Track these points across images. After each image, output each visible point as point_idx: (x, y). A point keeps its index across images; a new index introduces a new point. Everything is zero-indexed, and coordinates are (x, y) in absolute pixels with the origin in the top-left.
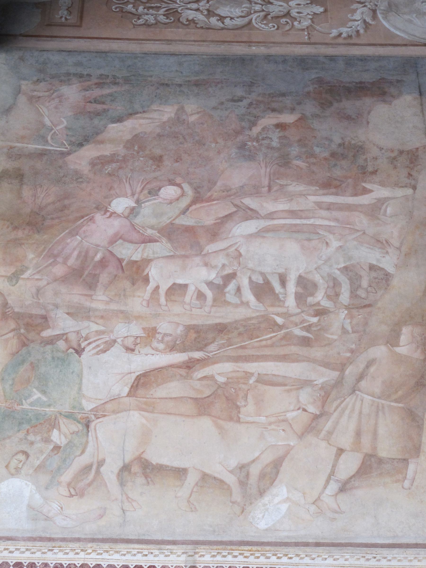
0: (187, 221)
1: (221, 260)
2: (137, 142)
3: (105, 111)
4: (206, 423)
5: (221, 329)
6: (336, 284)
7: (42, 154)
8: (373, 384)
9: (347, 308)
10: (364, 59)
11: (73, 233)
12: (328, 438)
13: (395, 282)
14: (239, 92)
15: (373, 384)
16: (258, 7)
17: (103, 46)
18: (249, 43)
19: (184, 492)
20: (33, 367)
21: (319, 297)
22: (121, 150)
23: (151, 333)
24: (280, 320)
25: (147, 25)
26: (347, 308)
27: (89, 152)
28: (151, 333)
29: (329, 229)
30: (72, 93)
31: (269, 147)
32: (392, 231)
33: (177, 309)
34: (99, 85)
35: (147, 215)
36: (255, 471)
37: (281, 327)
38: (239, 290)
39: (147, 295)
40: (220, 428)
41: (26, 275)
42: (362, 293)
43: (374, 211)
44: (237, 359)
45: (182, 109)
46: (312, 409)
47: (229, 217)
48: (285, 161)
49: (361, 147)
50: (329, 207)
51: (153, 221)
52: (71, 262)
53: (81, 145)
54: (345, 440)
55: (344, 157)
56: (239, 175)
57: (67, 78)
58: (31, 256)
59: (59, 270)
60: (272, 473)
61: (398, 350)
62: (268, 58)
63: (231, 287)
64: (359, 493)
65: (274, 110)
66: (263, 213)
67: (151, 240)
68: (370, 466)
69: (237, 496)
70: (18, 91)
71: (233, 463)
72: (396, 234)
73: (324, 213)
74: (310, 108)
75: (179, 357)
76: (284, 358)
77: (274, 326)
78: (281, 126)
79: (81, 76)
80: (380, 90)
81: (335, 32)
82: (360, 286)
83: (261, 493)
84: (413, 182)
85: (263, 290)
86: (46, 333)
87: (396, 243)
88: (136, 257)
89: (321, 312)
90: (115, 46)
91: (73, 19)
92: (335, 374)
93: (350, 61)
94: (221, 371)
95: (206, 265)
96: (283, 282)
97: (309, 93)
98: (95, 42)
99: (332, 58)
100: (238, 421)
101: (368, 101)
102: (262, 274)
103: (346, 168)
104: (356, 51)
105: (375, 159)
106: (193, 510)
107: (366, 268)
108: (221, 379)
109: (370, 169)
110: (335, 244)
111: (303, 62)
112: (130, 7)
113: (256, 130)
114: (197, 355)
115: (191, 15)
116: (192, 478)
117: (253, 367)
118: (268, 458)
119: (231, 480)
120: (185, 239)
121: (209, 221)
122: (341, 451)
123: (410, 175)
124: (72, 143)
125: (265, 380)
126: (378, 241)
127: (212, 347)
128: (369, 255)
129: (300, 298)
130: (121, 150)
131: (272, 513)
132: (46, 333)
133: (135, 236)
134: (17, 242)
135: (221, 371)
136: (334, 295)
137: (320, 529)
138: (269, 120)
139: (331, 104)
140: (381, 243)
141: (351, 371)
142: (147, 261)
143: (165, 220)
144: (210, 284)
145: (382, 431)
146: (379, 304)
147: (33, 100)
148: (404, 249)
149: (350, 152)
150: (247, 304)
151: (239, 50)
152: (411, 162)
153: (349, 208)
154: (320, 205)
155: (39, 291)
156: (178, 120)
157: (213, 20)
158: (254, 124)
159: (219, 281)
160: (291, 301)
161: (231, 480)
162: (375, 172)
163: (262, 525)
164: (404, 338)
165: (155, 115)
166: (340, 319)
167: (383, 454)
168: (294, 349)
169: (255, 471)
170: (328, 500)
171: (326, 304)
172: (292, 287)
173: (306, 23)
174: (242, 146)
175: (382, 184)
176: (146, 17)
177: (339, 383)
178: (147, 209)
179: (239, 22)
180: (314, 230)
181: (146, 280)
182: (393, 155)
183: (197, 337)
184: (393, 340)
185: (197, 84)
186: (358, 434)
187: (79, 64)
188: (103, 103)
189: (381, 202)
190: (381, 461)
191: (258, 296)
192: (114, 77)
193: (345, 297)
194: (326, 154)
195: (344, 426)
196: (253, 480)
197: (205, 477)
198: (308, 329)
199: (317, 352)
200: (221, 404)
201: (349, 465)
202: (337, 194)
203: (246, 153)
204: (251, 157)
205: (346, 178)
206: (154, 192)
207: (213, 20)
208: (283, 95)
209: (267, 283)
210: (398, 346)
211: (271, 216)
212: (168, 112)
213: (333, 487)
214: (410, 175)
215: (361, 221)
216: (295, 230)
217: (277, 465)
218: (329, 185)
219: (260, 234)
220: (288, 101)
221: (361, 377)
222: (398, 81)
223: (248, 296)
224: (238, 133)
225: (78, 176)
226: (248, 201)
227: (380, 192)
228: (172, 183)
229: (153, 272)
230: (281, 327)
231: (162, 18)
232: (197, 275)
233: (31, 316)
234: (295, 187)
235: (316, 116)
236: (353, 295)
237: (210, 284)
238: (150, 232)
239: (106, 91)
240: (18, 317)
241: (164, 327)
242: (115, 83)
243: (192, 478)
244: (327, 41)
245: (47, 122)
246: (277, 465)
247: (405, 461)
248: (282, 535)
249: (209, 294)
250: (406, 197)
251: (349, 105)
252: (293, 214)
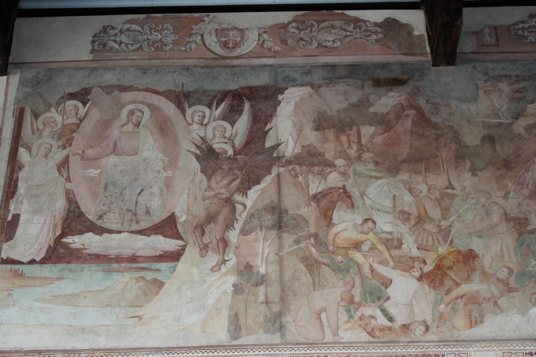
3: (524, 97)
7: (500, 125)
11: (527, 170)
17: (512, 56)
20: (528, 247)
25: (531, 42)
27: (522, 123)
30: (504, 86)
34: (517, 81)
41: (511, 195)
52: (530, 187)
53: (517, 118)
57: (499, 78)
58: (510, 184)
59: (526, 192)
70: (477, 88)
79: (506, 76)
86: (529, 228)
90: (519, 56)
91: (493, 41)
98: (508, 55)
112: (520, 31)
124: (512, 118)
132: (529, 228)
134: (501, 177)
147: (487, 92)
155: (520, 205)
176: (530, 38)
187: (503, 69)
188: (521, 92)
192: (523, 76)
225: (520, 136)
233: (520, 219)
239: (521, 85)
240: (514, 219)
242: (525, 80)
245: (498, 106)
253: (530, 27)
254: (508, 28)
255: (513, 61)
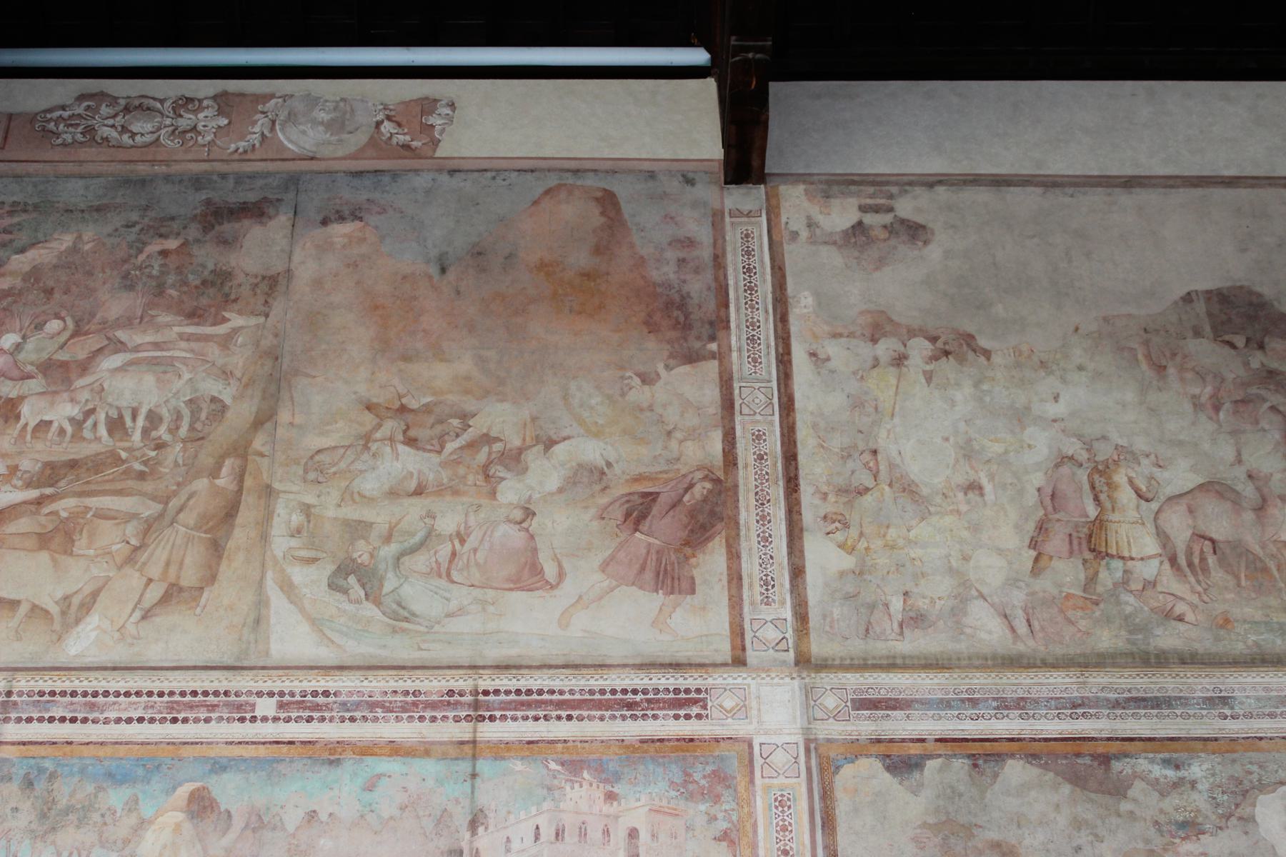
0: (63, 356)
1: (85, 395)
2: (34, 274)
3: (11, 241)
4: (44, 556)
5: (73, 465)
6: (179, 417)
8: (189, 517)
9: (183, 441)
10: (253, 176)
12: (141, 570)
13: (229, 415)
14: (134, 217)
15: (189, 517)
16: (168, 122)
18: (153, 162)
19: (13, 623)
21: (162, 432)
22: (18, 282)
23: (14, 469)
24: (124, 455)
25: (64, 145)
26: (183, 441)
28: (14, 469)
29: (184, 361)
31: (150, 276)
32: (239, 360)
33: (39, 446)
35: (30, 353)
36: (76, 601)
37: (124, 462)
38: (95, 425)
39: (16, 433)
40: (54, 560)
42: (198, 426)
43: (226, 342)
44: (81, 494)
45: (80, 237)
46: (134, 542)
47: (100, 350)
48: (160, 290)
49: (230, 273)
50: (189, 338)
51: (33, 357)
54: (155, 571)
55: (213, 284)
56: (116, 305)
60: (87, 606)
61: (218, 482)
62: (167, 178)
63: (89, 422)
64: (157, 620)
65: (161, 236)
66: (130, 345)
67: (29, 377)
68: (173, 594)
69: (57, 626)
71: (59, 594)
72: (241, 364)
73: (183, 344)
74: (193, 232)
75: (33, 494)
76: (120, 493)
77: (118, 461)
78: (164, 253)
80: (257, 211)
81: (233, 146)
82: (198, 419)
83: (78, 621)
84: (267, 309)
85: (116, 426)
87: (238, 374)
88: (13, 395)
89: (160, 446)
90: (32, 168)
92: (160, 507)
93: (240, 179)
94: (65, 506)
95: (72, 400)
96: (134, 418)
97: (195, 216)
98: (14, 165)
99: (224, 176)
100: (71, 554)
101: (246, 222)
102: (118, 408)
103: (209, 296)
104: (248, 168)
105: (240, 285)
106: (19, 639)
107: (208, 400)
108: (64, 514)
109: (233, 297)
110: (187, 376)
111: (198, 182)
112: (53, 124)
113: (142, 257)
114: (48, 491)
115: (106, 131)
116: (24, 609)
117: (94, 502)
118: (88, 590)
119: (54, 610)
120: (59, 373)
121: (82, 355)
122: (150, 580)
123: (266, 302)
125: (102, 515)
126: (224, 372)
127: (62, 483)
128: (212, 387)
129: (145, 432)
130: (18, 282)
131: (83, 643)
133: (16, 373)
135: (65, 506)
136: (173, 430)
137: (120, 654)
138: (155, 247)
139: (213, 227)
140: (226, 374)
141: (174, 503)
142: (21, 398)
143: (45, 356)
144: (71, 420)
145: (188, 560)
146: (211, 437)
148: (245, 380)
149: (221, 278)
150: (98, 439)
151: (142, 169)
152: (271, 288)
153: (206, 338)
154: (182, 337)
156: (74, 249)
157: (125, 137)
158: (140, 251)
159: (80, 417)
160: (137, 436)
161: (54, 610)
162: (235, 300)
163: (73, 652)
164: (224, 471)
165: (54, 244)
166: (175, 452)
167: (184, 583)
168: (130, 483)
169: (76, 601)
170: (131, 628)
171: (167, 437)
172: (141, 422)
173: (208, 138)
174: (126, 276)
175: (240, 313)
176: (64, 136)
177: (161, 515)
178: (30, 346)
179: (148, 138)
180: (171, 362)
181: (18, 417)
182: (255, 281)
183: (52, 474)
184: (215, 473)
185: (98, 209)
186: (168, 564)
188: (10, 233)
189: (236, 331)
190: (181, 590)
191: (111, 432)
192: (26, 204)
193: (183, 431)
194: (198, 282)
195: (158, 555)
196: (74, 608)
197: (34, 607)
198: (145, 463)
199: (148, 486)
200: (59, 539)
201: (155, 593)
202: (198, 324)
203: (128, 284)
204: (131, 288)
205: (210, 306)
206: (39, 327)
207: (125, 137)
208: (173, 219)
209: (121, 417)
210: (218, 477)
211: (137, 349)
212: (67, 240)
213: (138, 614)
214: (266, 302)
215: (213, 351)
216: (154, 362)
217: (95, 595)
218: (194, 315)
219: (121, 369)
220: (175, 225)
221: (181, 510)
222: (278, 200)
223: (102, 431)
224: (125, 261)
226: (121, 335)
227: (236, 320)
228: (57, 316)
229: (25, 409)
230: (124, 462)
231: (79, 137)
232: (63, 411)
234: (164, 318)
235: (197, 241)
236: (192, 428)
237: (71, 420)
238: (29, 368)
239: (16, 220)
241: (25, 464)
242: (25, 211)
243: (24, 609)
244: (224, 157)
246: (95, 595)
247: (202, 588)
248: (89, 660)
249: (69, 429)
250: (257, 326)
251: (227, 228)
252: (157, 346)
253: (70, 117)
254: (33, 118)
255: (17, 177)
